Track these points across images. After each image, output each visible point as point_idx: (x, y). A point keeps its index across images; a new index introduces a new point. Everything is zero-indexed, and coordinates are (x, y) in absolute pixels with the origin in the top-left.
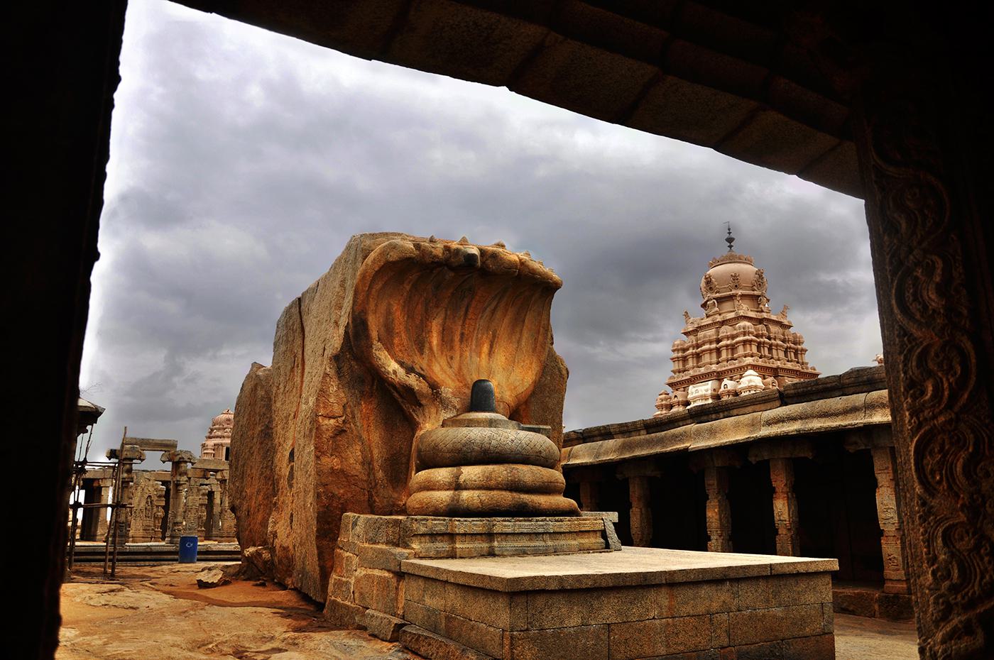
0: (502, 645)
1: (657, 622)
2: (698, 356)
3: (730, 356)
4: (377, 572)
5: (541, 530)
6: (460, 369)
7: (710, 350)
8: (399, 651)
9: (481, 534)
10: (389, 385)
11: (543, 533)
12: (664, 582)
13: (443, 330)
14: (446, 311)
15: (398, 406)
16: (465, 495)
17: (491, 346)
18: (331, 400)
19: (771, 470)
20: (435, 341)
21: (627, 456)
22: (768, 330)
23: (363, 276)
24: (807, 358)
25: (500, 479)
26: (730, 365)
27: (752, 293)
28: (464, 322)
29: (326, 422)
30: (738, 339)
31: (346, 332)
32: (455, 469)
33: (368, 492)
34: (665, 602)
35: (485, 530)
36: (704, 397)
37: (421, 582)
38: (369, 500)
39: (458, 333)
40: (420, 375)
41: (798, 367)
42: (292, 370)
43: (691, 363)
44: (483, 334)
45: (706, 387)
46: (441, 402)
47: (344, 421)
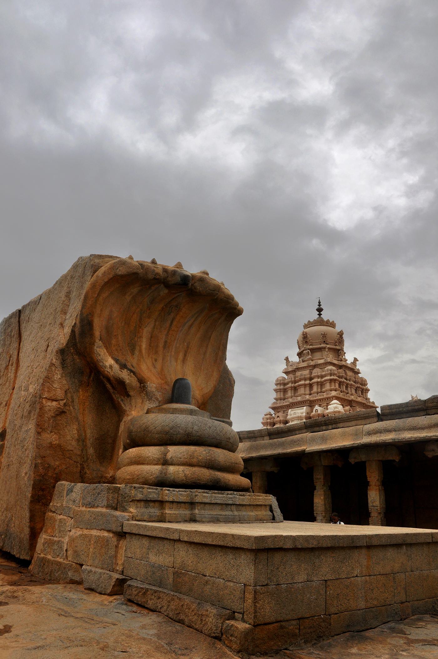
0: (243, 599)
1: (359, 579)
2: (295, 389)
3: (319, 390)
4: (95, 533)
5: (230, 502)
6: (162, 369)
7: (305, 385)
8: (122, 604)
9: (184, 503)
10: (104, 377)
11: (231, 505)
12: (365, 544)
13: (151, 337)
14: (155, 321)
15: (108, 394)
16: (172, 469)
17: (185, 355)
18: (55, 386)
19: (367, 469)
20: (144, 346)
21: (254, 455)
22: (346, 373)
23: (93, 286)
24: (370, 395)
25: (200, 458)
26: (320, 396)
27: (335, 347)
28: (168, 332)
29: (49, 403)
30: (326, 378)
31: (73, 331)
32: (162, 448)
33: (81, 465)
34: (364, 562)
35: (188, 500)
36: (300, 418)
37: (145, 542)
38: (81, 472)
40: (131, 371)
41: (364, 402)
42: (7, 368)
43: (289, 394)
45: (302, 411)
46: (147, 394)
47: (65, 404)
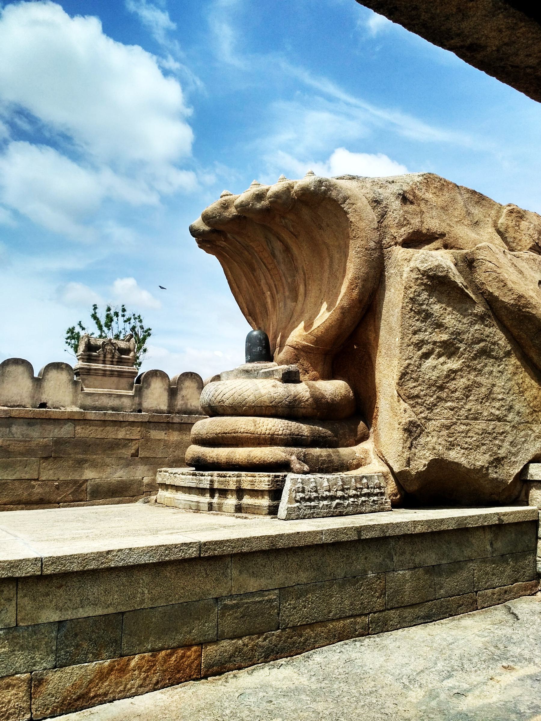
17: (305, 286)
44: (294, 276)
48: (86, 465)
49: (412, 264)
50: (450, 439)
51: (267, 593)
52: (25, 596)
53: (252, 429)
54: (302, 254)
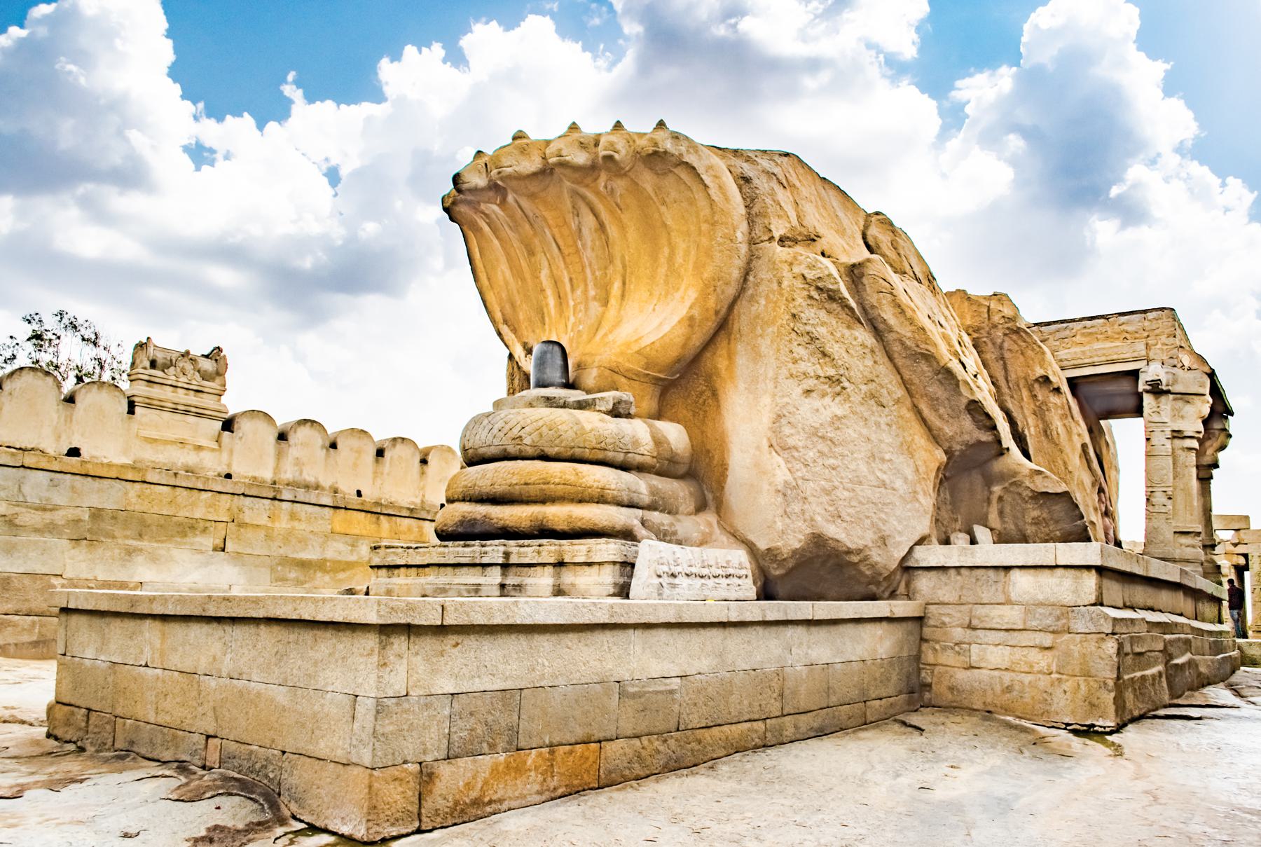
17: (624, 283)
39: (567, 281)
44: (606, 268)
48: (140, 559)
49: (796, 270)
50: (831, 509)
51: (668, 681)
52: (417, 654)
53: (572, 478)
54: (627, 238)
